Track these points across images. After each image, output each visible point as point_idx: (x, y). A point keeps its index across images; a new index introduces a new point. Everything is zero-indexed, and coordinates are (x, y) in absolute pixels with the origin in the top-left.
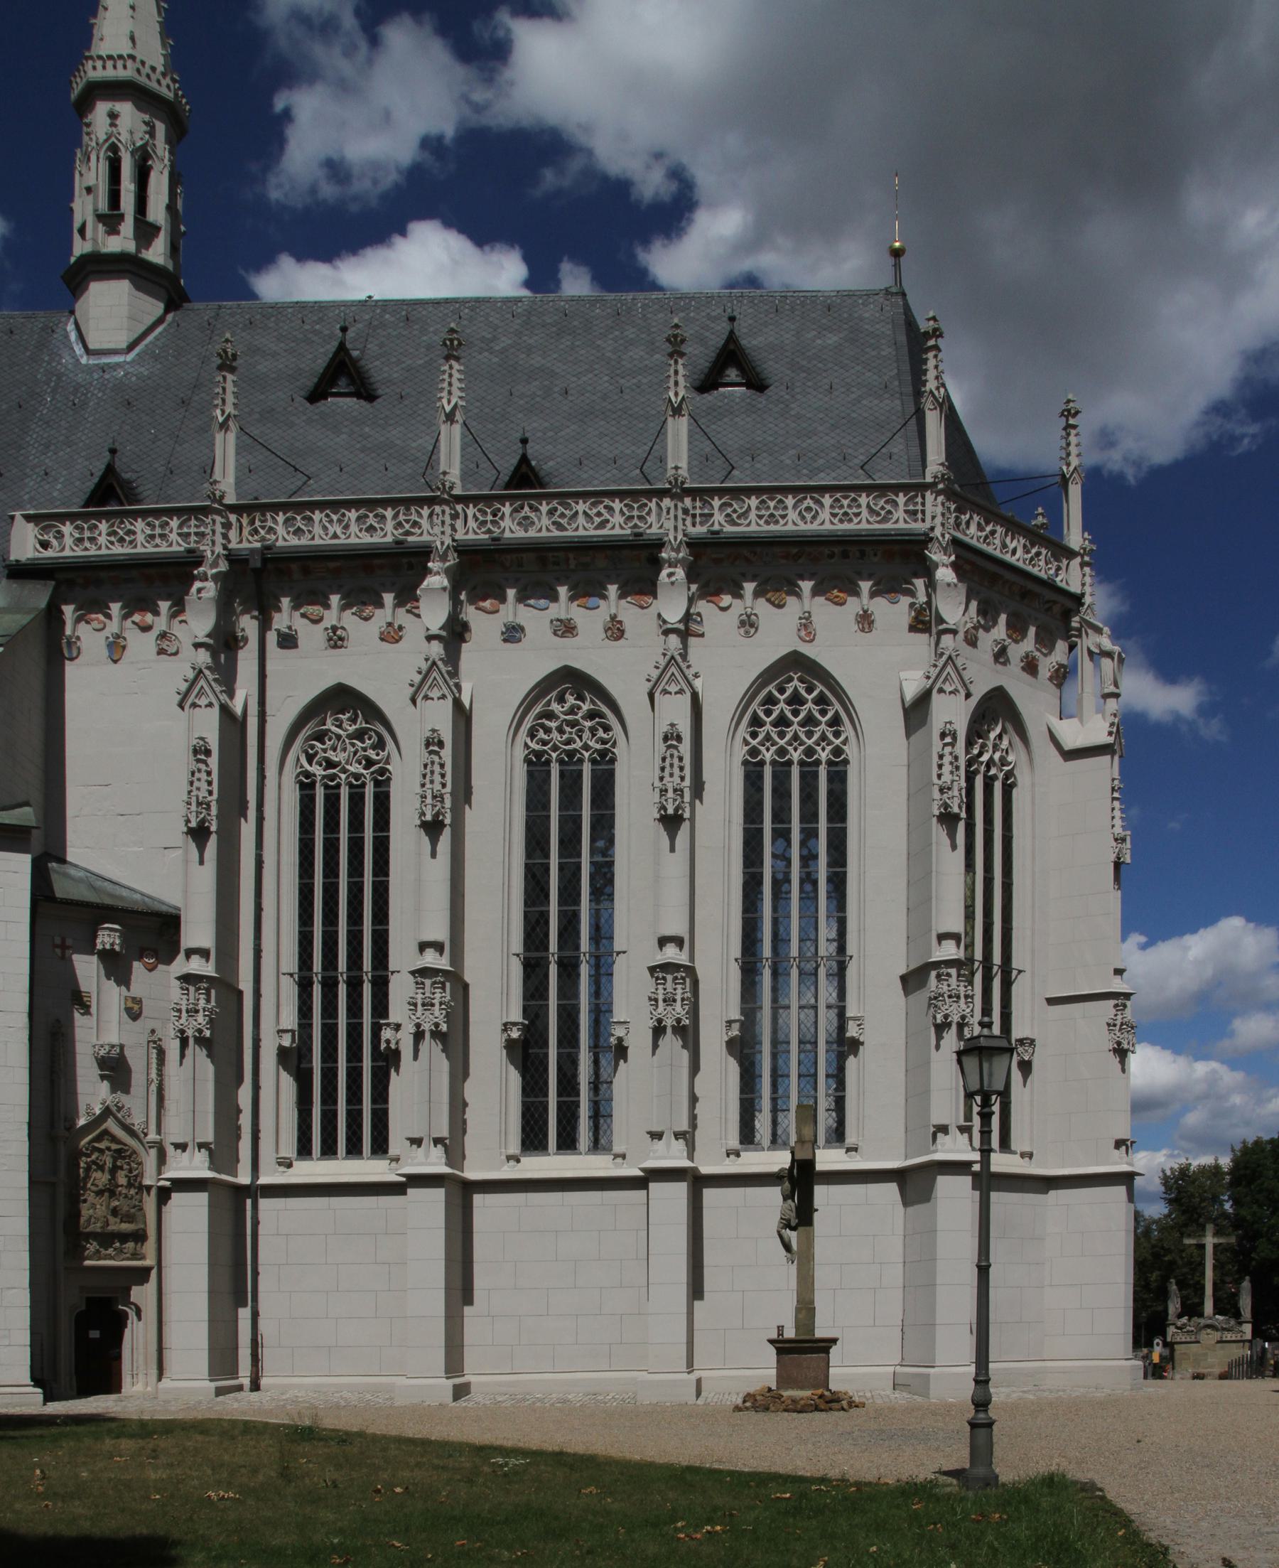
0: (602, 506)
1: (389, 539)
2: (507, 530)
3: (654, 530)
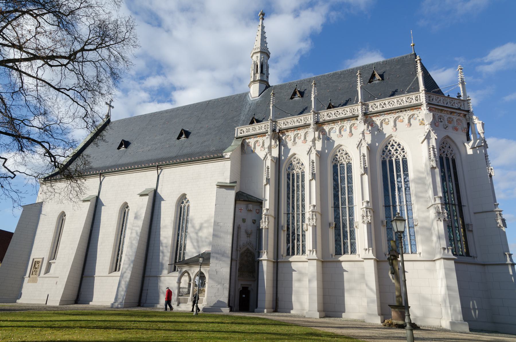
1: (303, 123)
3: (357, 113)
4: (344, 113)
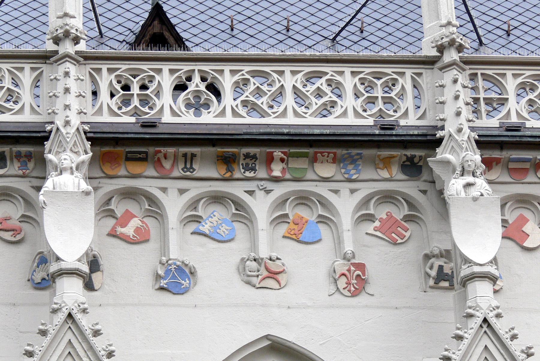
0: (323, 80)
2: (167, 111)
3: (412, 120)
4: (316, 103)
